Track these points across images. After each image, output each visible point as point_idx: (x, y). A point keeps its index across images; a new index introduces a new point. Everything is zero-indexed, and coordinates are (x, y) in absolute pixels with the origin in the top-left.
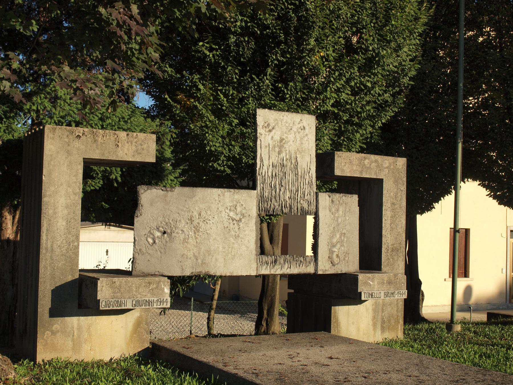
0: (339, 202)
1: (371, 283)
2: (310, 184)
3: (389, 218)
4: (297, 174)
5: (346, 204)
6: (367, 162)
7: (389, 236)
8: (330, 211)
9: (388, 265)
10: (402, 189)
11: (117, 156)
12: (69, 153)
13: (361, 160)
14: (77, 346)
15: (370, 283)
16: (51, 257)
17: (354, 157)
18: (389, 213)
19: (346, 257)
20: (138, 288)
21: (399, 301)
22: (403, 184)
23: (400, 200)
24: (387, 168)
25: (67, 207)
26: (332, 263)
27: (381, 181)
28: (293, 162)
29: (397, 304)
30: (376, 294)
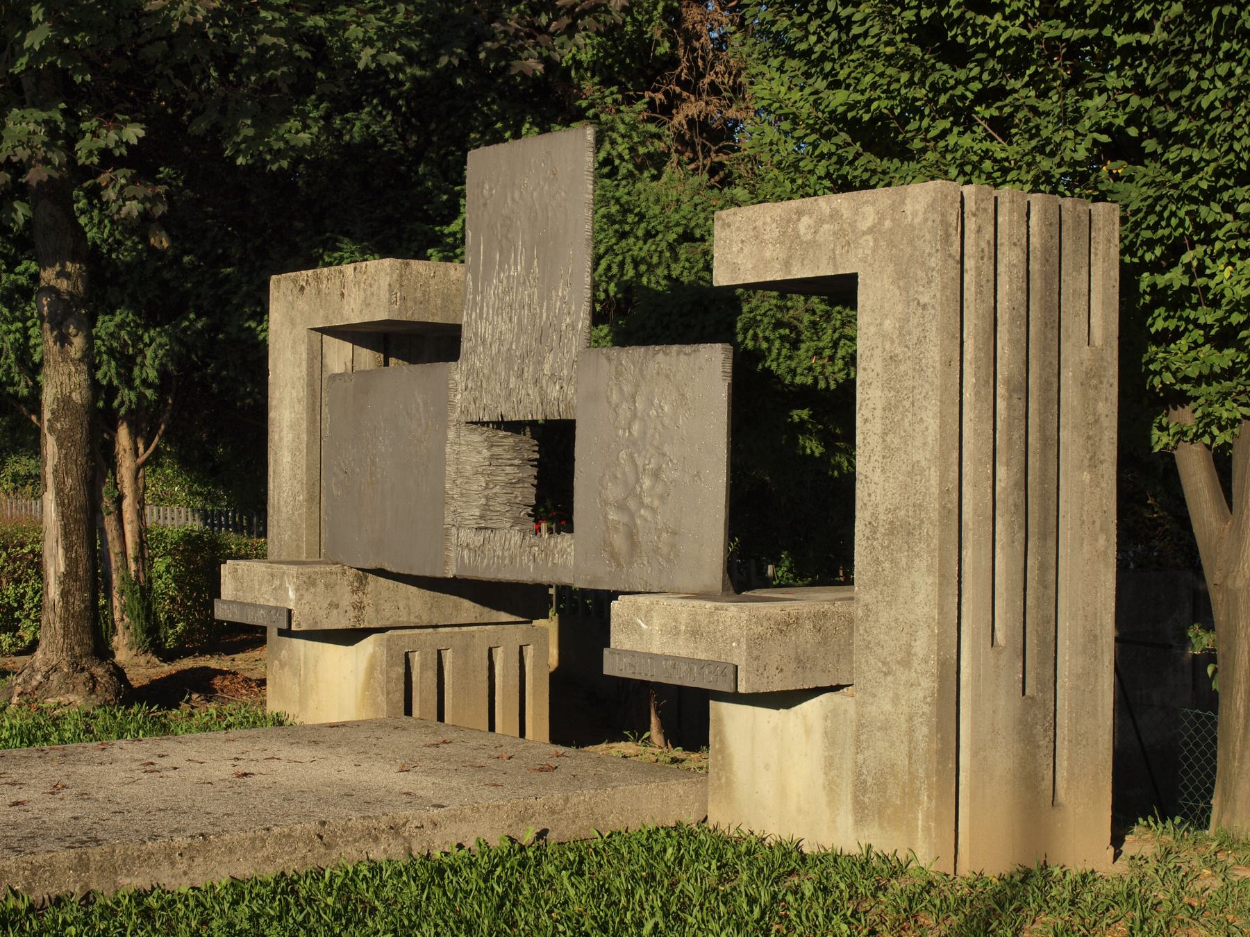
1: (643, 626)
3: (879, 413)
7: (877, 477)
9: (876, 583)
10: (924, 299)
13: (788, 221)
15: (640, 626)
17: (768, 215)
18: (879, 393)
21: (917, 720)
22: (929, 282)
23: (919, 342)
24: (871, 230)
29: (911, 731)
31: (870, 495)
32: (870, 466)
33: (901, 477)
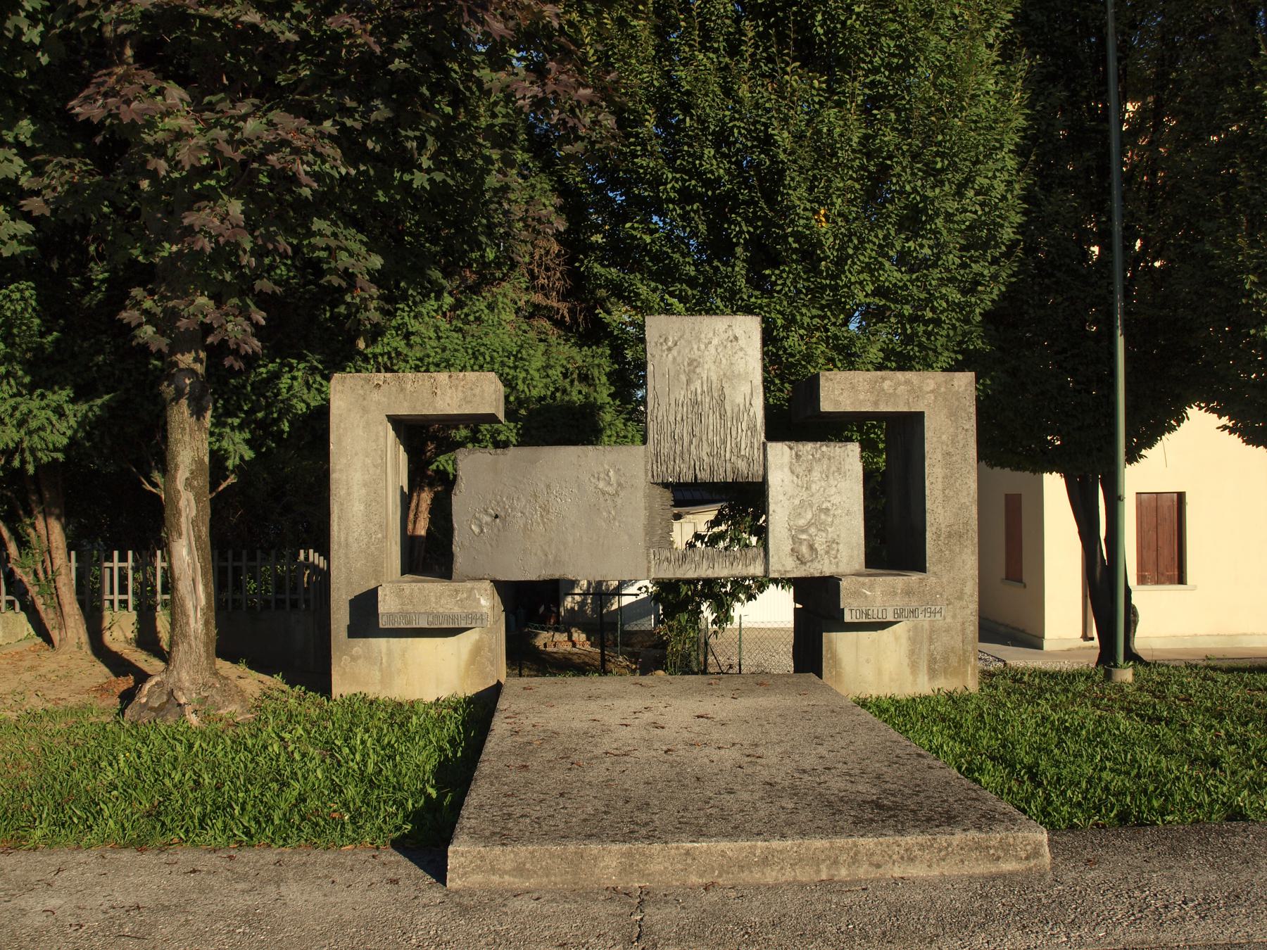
1: (868, 593)
2: (753, 429)
3: (940, 480)
4: (722, 416)
5: (829, 459)
6: (886, 384)
7: (940, 510)
8: (792, 472)
9: (940, 562)
10: (966, 427)
11: (435, 408)
12: (365, 410)
13: (876, 382)
14: (386, 678)
16: (346, 555)
17: (861, 378)
18: (940, 470)
20: (438, 598)
21: (967, 624)
22: (970, 419)
24: (932, 391)
25: (365, 485)
26: (801, 560)
27: (919, 416)
28: (716, 395)
29: (963, 630)
30: (876, 612)
32: (935, 505)
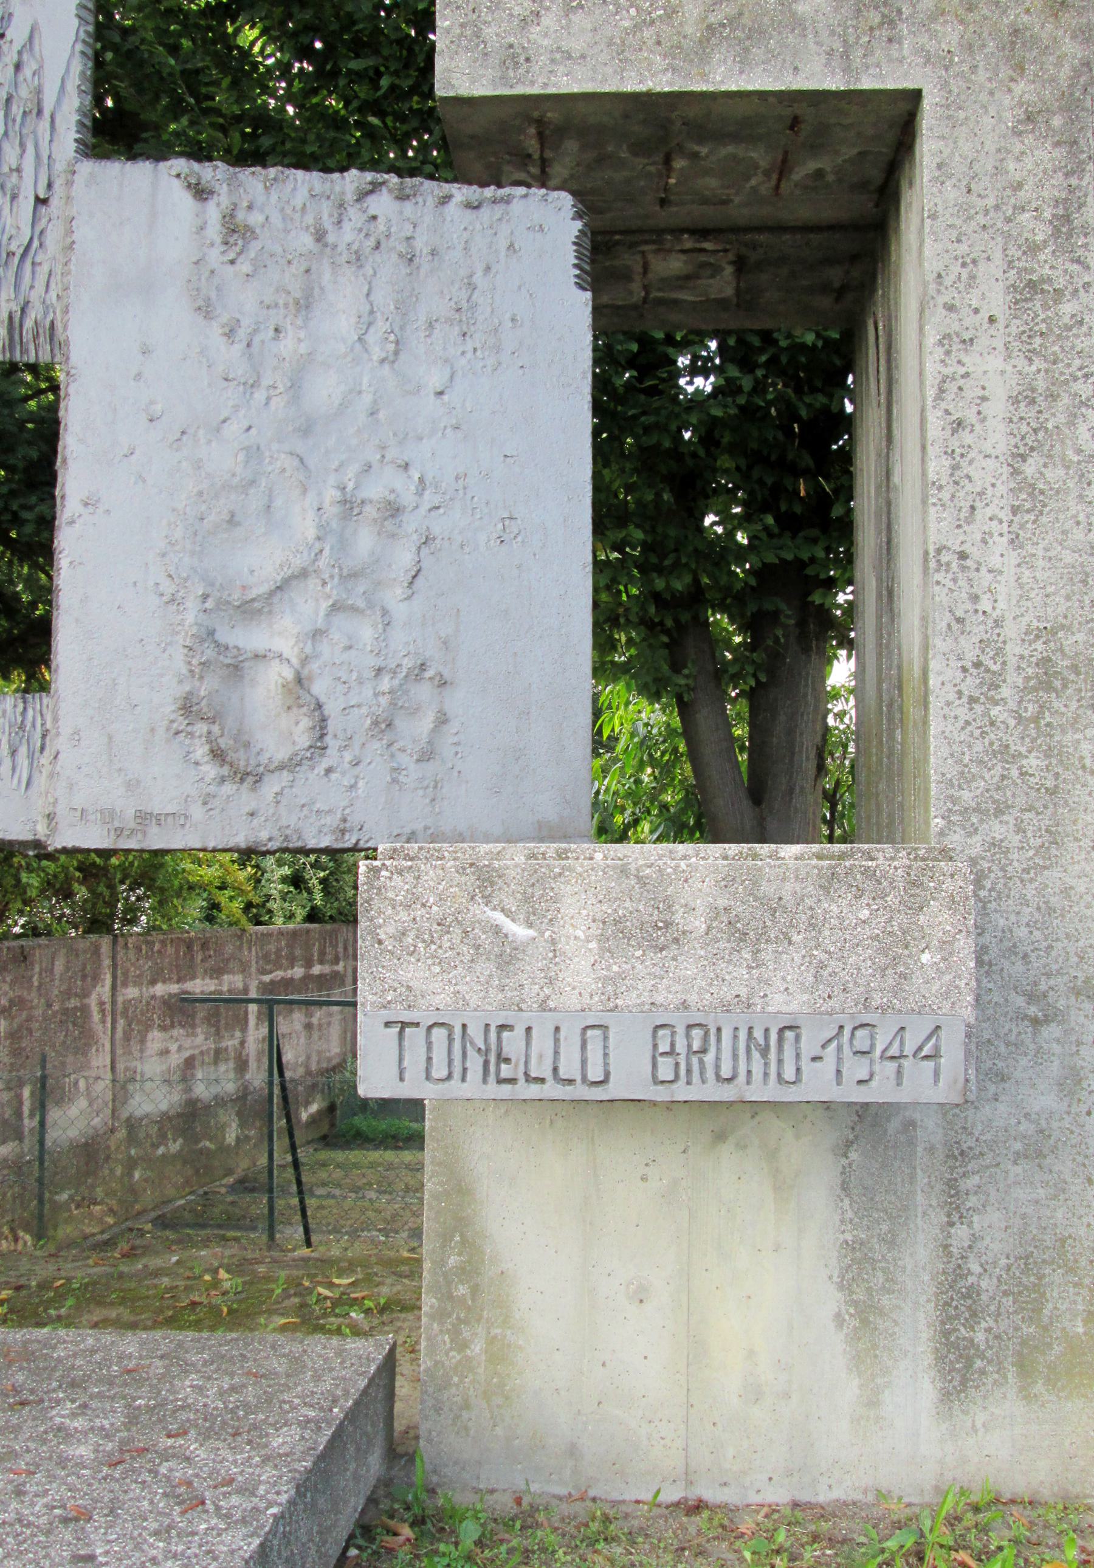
0: (320, 236)
1: (519, 931)
3: (998, 407)
8: (206, 310)
15: (497, 930)
18: (996, 362)
19: (415, 711)
30: (542, 1043)
31: (975, 598)
32: (975, 532)
33: (1068, 557)
